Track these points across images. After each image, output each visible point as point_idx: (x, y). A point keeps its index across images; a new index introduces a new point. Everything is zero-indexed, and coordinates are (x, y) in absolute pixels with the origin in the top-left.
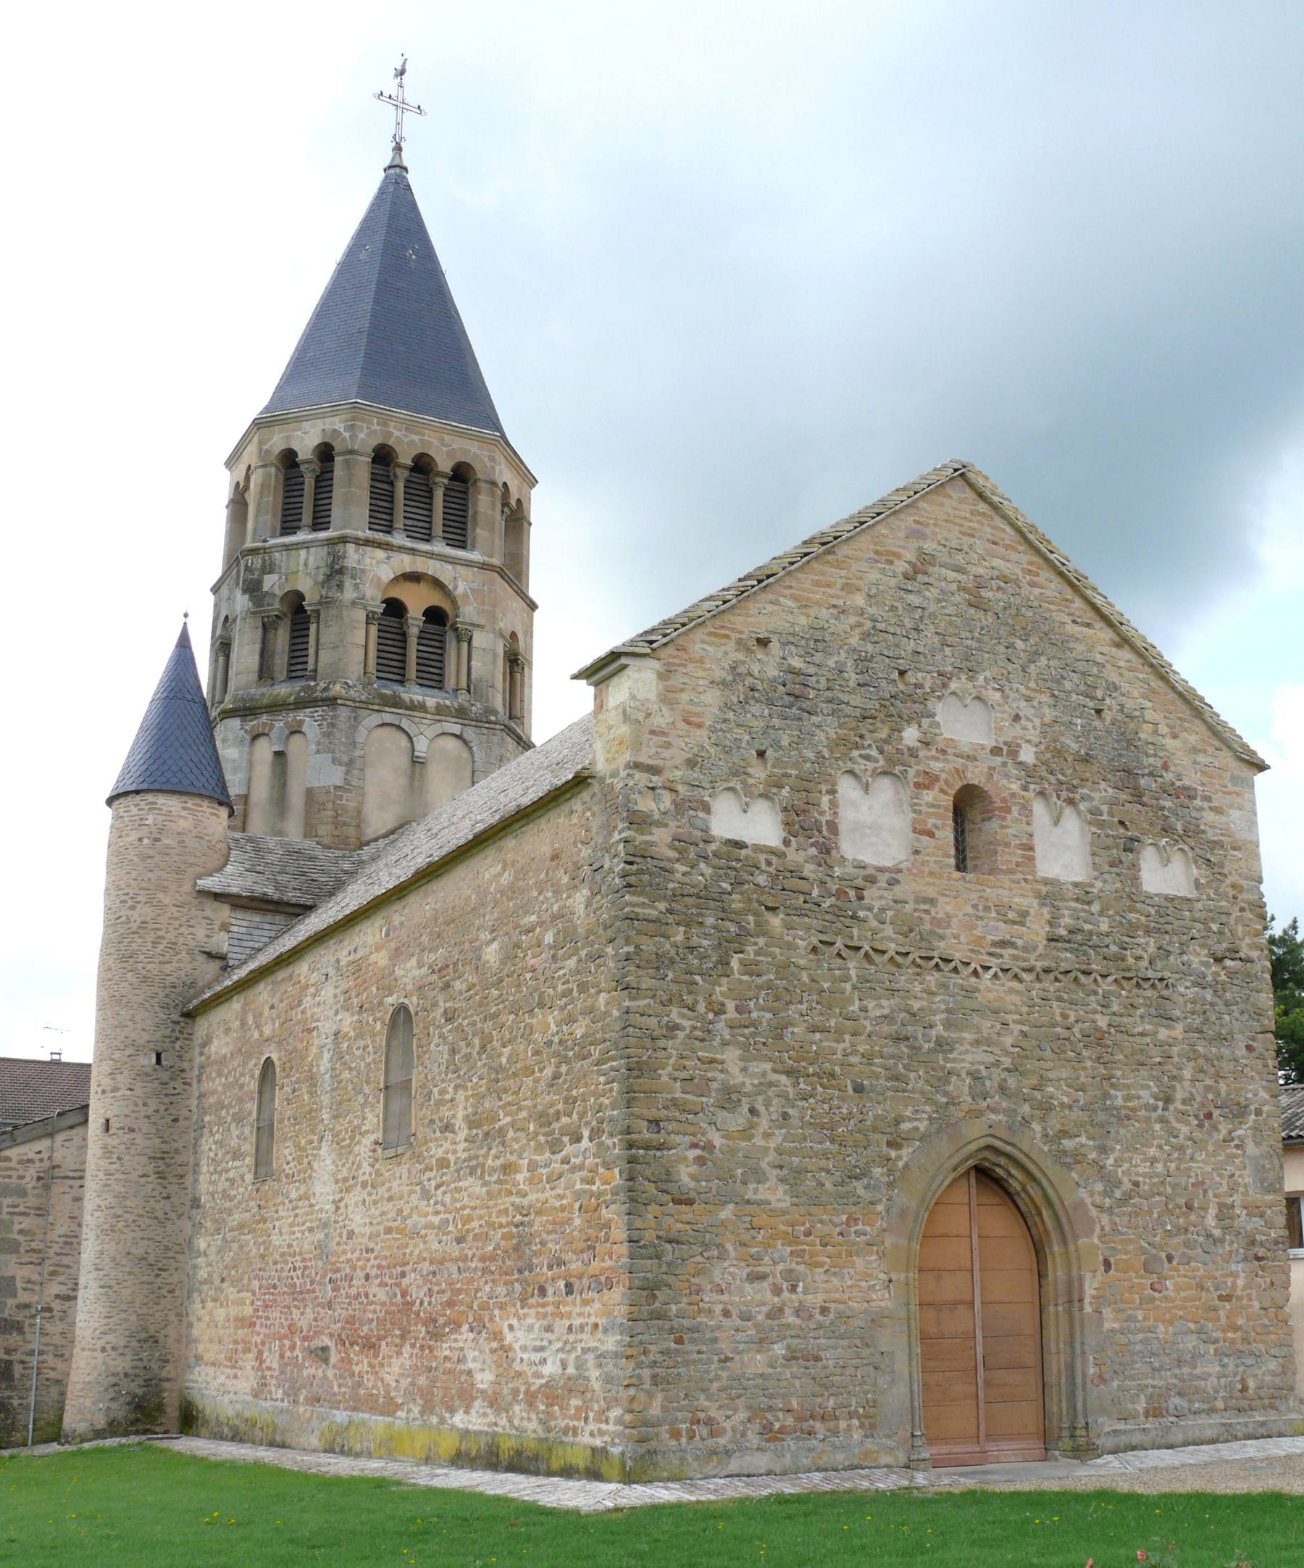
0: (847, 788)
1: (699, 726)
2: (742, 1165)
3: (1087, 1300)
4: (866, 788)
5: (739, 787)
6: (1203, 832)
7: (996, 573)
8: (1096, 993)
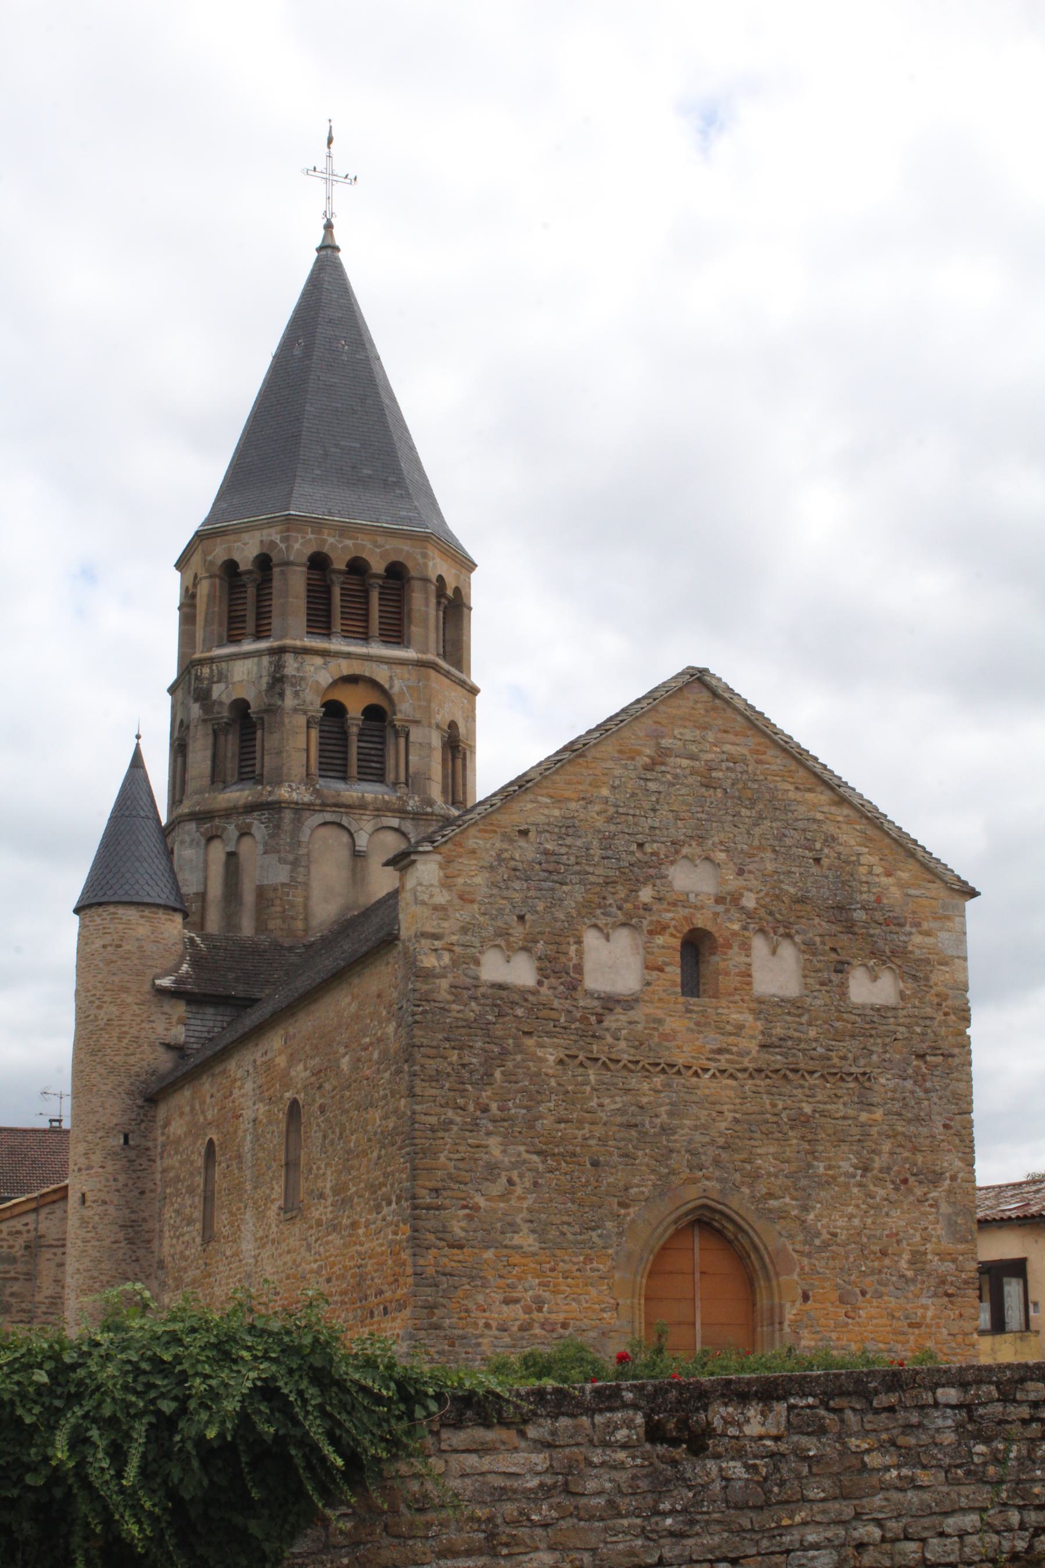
0: (591, 939)
1: (472, 902)
2: (500, 1220)
3: (786, 1323)
4: (607, 938)
5: (503, 944)
6: (911, 952)
7: (725, 756)
8: (802, 1086)
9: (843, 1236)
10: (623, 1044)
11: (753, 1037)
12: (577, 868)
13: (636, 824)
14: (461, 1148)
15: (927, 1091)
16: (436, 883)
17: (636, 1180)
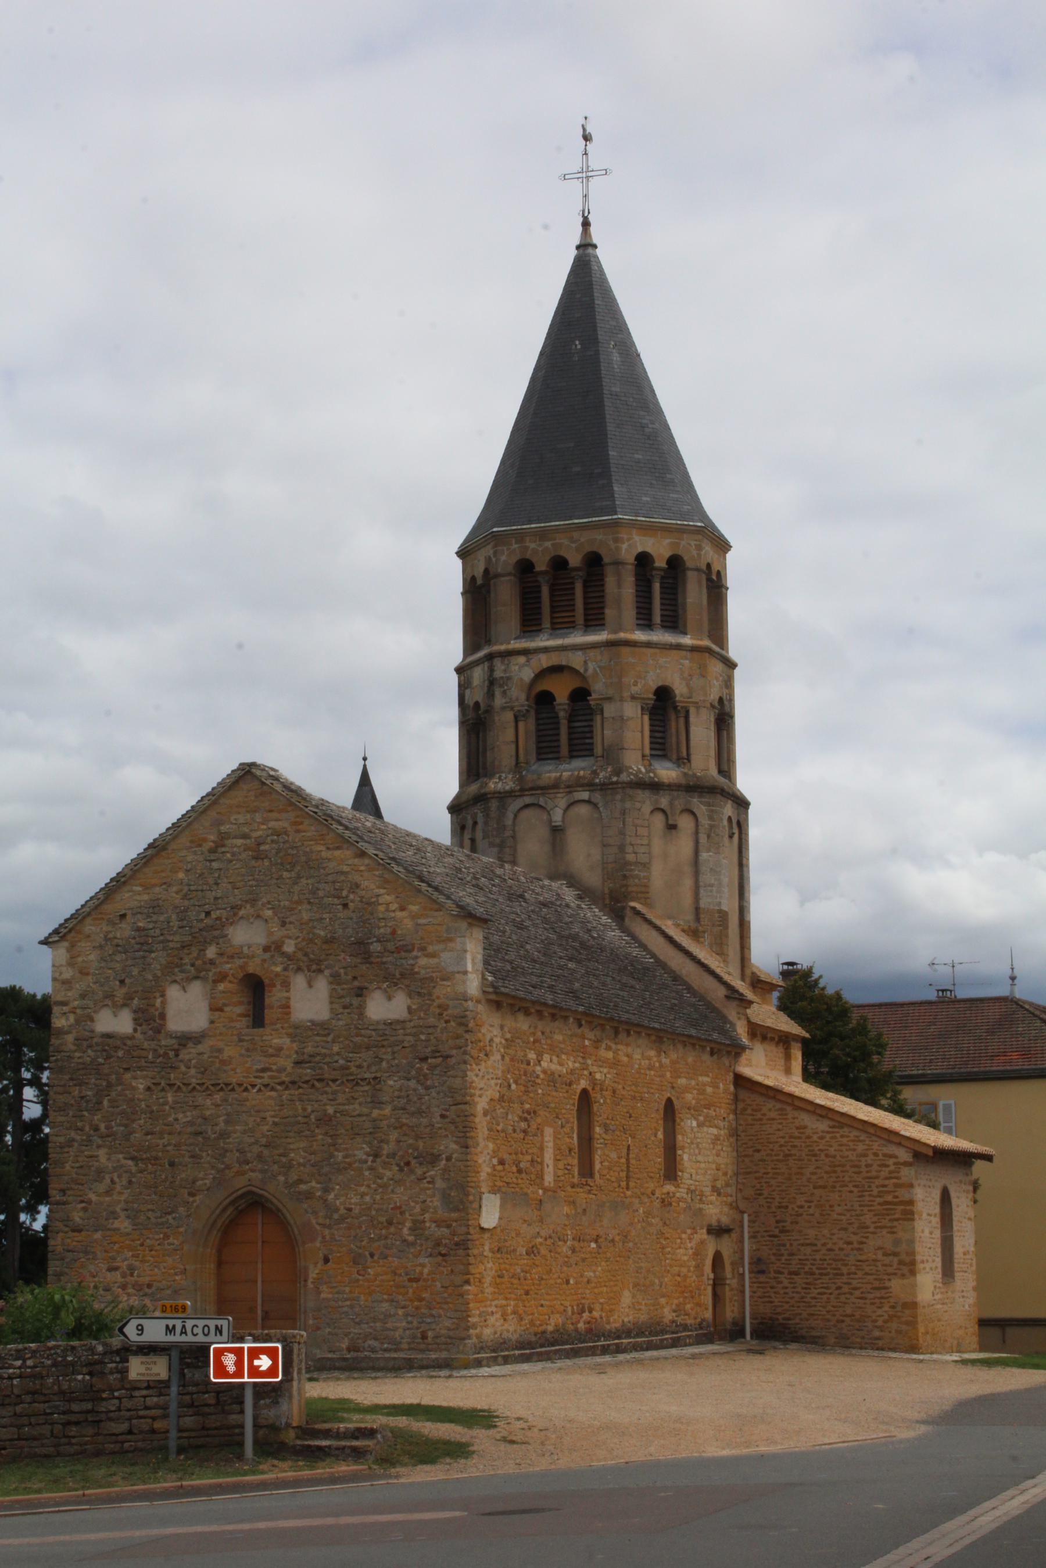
0: (173, 992)
1: (87, 974)
3: (310, 1280)
4: (184, 989)
6: (417, 973)
7: (270, 832)
8: (326, 1093)
9: (356, 1211)
10: (193, 1071)
12: (162, 938)
13: (204, 897)
14: (80, 1159)
16: (64, 963)
17: (201, 1175)
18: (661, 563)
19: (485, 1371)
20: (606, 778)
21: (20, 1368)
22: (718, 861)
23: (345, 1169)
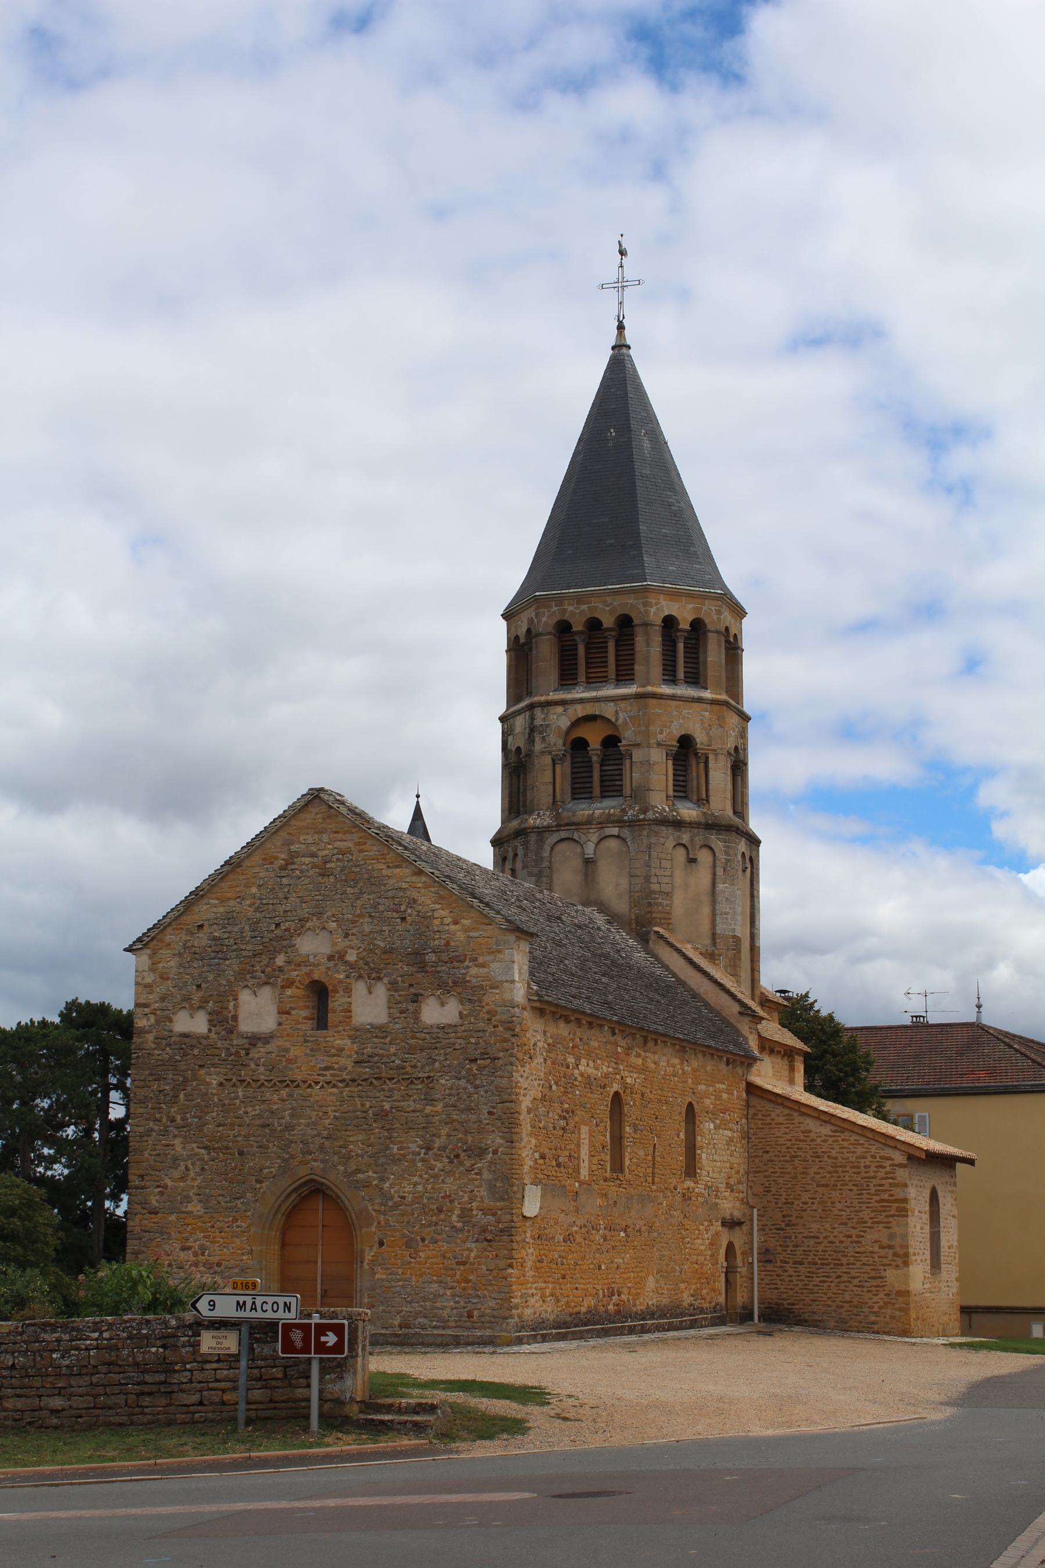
0: (245, 996)
1: (168, 979)
2: (180, 1194)
3: (366, 1262)
4: (255, 993)
6: (468, 981)
7: (336, 851)
8: (383, 1090)
10: (262, 1069)
11: (350, 1056)
12: (235, 947)
13: (274, 910)
15: (476, 1087)
18: (685, 625)
19: (526, 1348)
20: (633, 815)
21: (96, 1339)
22: (732, 891)
23: (399, 1160)
